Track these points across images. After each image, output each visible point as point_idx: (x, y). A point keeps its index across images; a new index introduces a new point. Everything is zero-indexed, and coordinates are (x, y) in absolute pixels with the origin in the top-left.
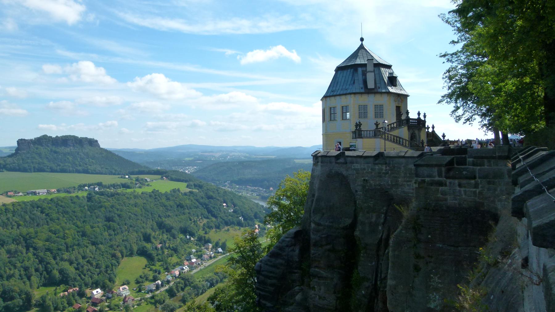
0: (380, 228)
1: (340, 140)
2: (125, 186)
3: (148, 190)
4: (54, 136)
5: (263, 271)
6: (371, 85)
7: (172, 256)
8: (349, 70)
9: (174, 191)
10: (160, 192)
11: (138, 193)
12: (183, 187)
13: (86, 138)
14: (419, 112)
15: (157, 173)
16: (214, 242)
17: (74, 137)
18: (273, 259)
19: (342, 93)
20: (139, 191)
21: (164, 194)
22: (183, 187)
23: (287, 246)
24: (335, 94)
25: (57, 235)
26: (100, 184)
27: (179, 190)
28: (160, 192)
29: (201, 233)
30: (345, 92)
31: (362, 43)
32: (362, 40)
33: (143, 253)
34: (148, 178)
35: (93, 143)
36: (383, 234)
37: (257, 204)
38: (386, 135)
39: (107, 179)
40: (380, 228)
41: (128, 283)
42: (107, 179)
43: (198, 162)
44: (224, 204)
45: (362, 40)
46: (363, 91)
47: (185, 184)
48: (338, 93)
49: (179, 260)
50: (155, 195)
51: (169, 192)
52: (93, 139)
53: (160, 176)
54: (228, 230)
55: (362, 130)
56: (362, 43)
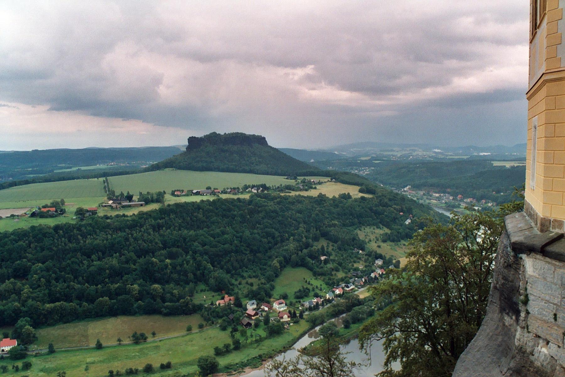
3: (313, 193)
4: (222, 133)
7: (337, 270)
12: (354, 192)
17: (242, 134)
22: (354, 192)
25: (217, 239)
26: (264, 187)
35: (261, 140)
41: (285, 297)
47: (358, 188)
50: (322, 199)
52: (261, 136)
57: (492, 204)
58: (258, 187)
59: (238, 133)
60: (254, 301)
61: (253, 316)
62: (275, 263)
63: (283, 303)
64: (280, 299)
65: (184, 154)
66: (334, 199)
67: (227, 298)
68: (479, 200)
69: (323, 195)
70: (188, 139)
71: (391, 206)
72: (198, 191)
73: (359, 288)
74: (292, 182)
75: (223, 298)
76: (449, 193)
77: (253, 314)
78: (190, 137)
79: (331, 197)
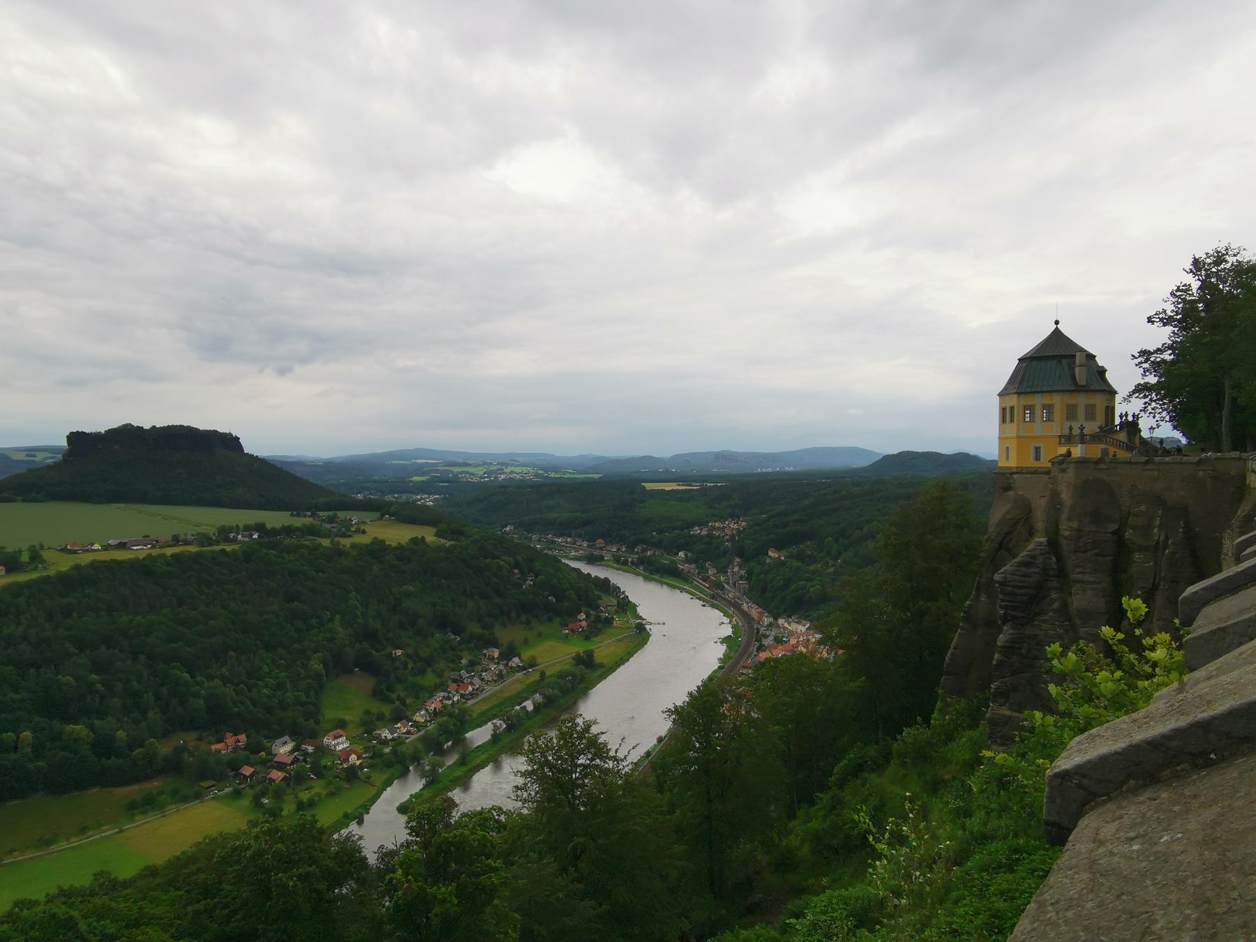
0: (1156, 530)
1: (1038, 445)
2: (311, 531)
4: (147, 427)
5: (1009, 582)
6: (1081, 381)
8: (1049, 362)
9: (414, 541)
10: (387, 543)
11: (344, 546)
12: (429, 535)
13: (215, 432)
14: (1134, 413)
15: (367, 506)
16: (502, 645)
18: (1023, 569)
19: (1044, 389)
20: (346, 542)
21: (396, 548)
22: (429, 535)
23: (1041, 554)
24: (1034, 390)
26: (260, 528)
27: (423, 538)
28: (387, 543)
29: (475, 628)
30: (1049, 389)
31: (1057, 327)
32: (1057, 323)
33: (367, 666)
34: (355, 517)
35: (231, 442)
36: (1160, 535)
37: (578, 571)
38: (1108, 439)
39: (276, 519)
40: (1156, 530)
42: (276, 519)
43: (441, 484)
44: (516, 571)
45: (1057, 323)
46: (1073, 388)
48: (1039, 389)
49: (438, 680)
50: (378, 550)
51: (404, 545)
52: (230, 434)
53: (378, 514)
54: (528, 623)
55: (1086, 435)
56: (1057, 327)
57: (652, 552)
58: (249, 529)
59: (182, 427)
60: (286, 738)
61: (290, 765)
62: (316, 665)
63: (342, 736)
64: (336, 729)
65: (55, 466)
66: (400, 547)
67: (230, 740)
68: (631, 548)
69: (381, 541)
70: (67, 437)
71: (498, 558)
72: (124, 541)
73: (469, 699)
74: (308, 521)
75: (220, 741)
76: (580, 536)
77: (289, 763)
78: (71, 433)
79: (394, 544)
